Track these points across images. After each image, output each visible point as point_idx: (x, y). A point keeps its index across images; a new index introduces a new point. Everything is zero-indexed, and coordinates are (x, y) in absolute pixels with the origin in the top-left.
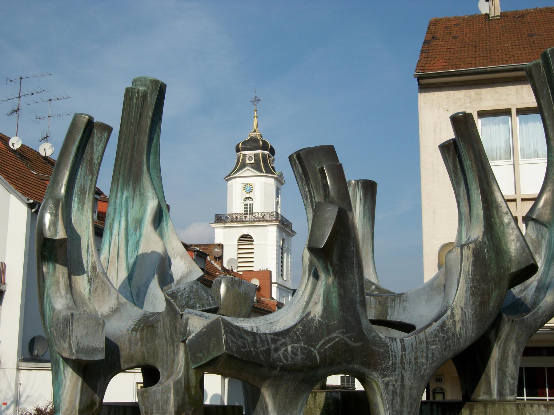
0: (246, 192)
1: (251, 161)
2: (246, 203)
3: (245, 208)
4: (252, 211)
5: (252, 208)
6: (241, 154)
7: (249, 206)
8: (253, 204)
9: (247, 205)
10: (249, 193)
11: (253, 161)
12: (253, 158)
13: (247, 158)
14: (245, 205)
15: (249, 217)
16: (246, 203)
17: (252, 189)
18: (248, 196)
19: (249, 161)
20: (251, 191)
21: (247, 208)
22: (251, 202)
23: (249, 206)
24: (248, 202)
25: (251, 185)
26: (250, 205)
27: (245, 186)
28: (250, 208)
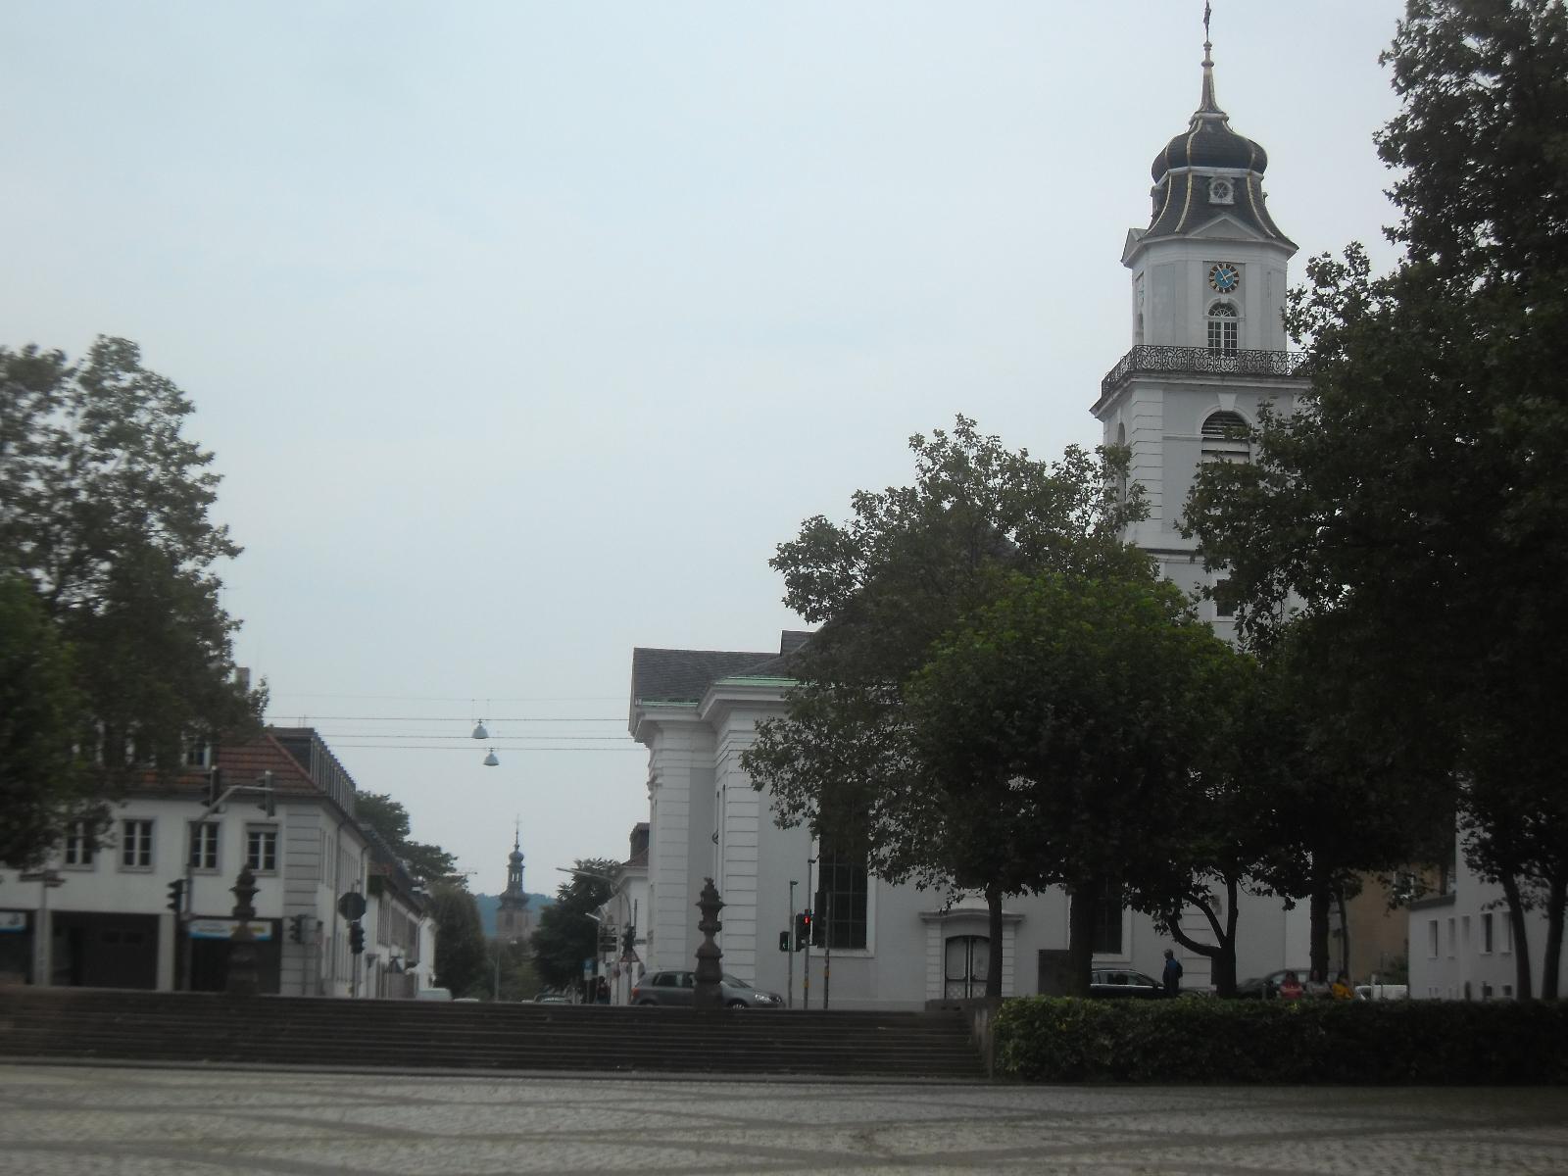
0: (1218, 289)
1: (1216, 194)
2: (1215, 319)
3: (1210, 335)
4: (1234, 344)
5: (1234, 336)
6: (1190, 171)
7: (1223, 330)
8: (1234, 326)
9: (1218, 325)
10: (1227, 291)
11: (1229, 200)
12: (1230, 186)
13: (1212, 186)
14: (1211, 325)
15: (1228, 364)
16: (1215, 319)
17: (1237, 282)
18: (1224, 298)
19: (1225, 195)
20: (1233, 288)
21: (1218, 335)
22: (1231, 319)
23: (1223, 330)
24: (1223, 319)
25: (1233, 270)
26: (1227, 326)
27: (1215, 269)
28: (1227, 335)
